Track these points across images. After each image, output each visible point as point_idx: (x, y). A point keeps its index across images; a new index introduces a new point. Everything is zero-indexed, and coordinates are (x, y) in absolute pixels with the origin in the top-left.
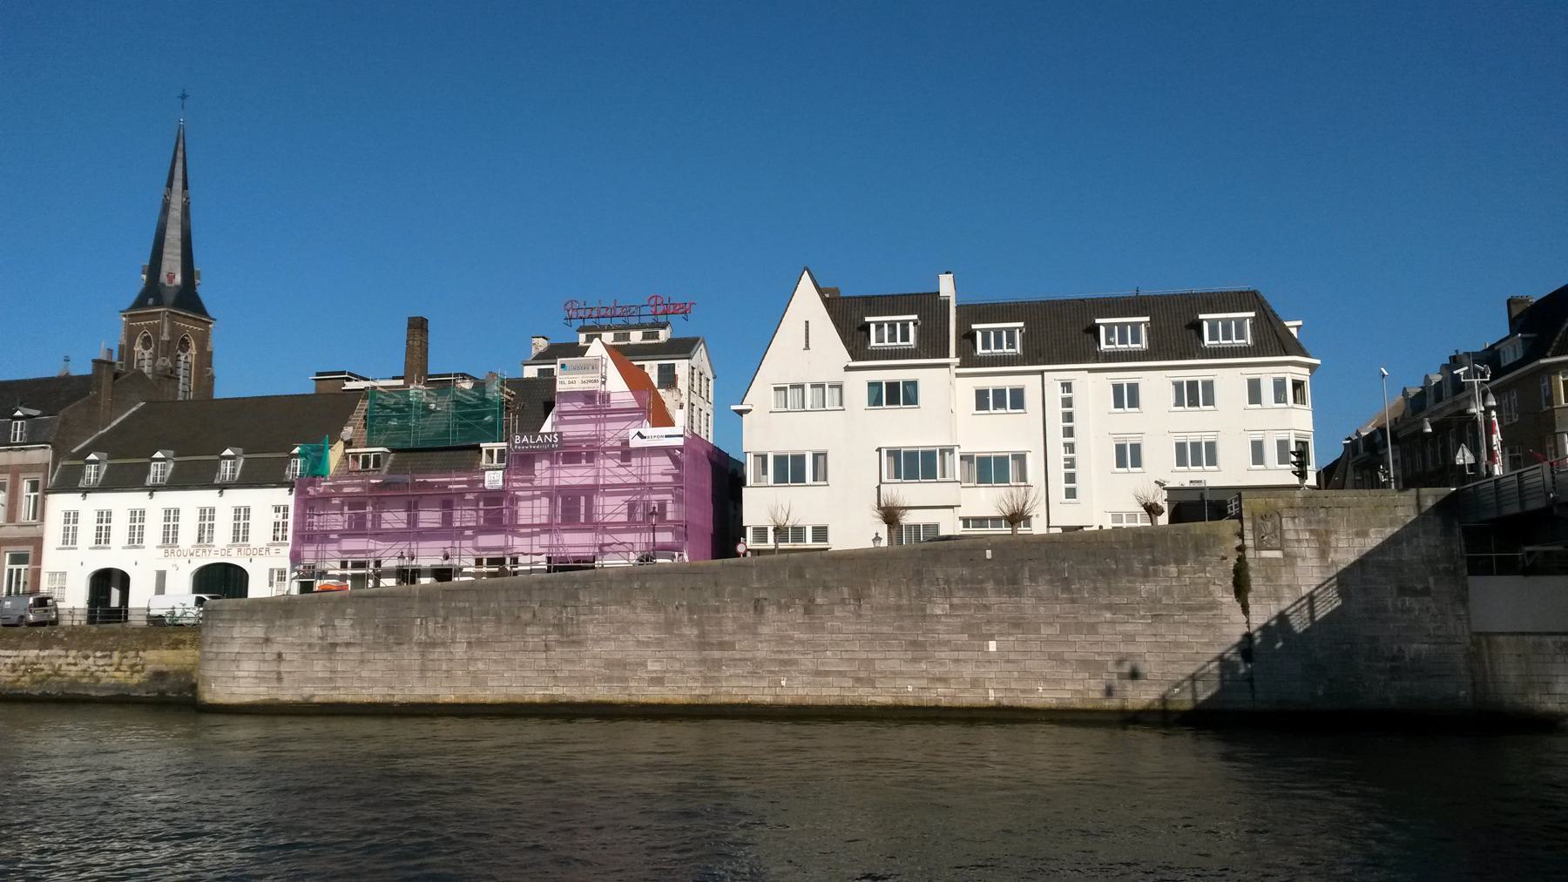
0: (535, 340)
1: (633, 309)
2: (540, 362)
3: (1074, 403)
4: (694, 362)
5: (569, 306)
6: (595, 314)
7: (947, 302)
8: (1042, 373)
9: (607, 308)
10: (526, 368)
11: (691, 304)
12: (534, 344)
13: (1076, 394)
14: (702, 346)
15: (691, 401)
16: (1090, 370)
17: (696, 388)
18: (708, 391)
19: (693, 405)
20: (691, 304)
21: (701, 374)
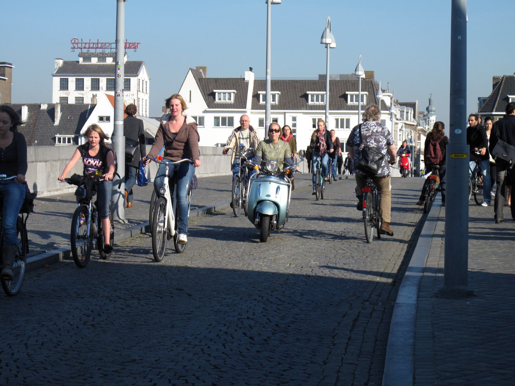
0: (57, 61)
1: (107, 45)
2: (61, 75)
3: (297, 125)
4: (139, 77)
5: (73, 42)
6: (87, 46)
7: (247, 84)
8: (285, 113)
9: (94, 44)
10: (54, 77)
11: (138, 44)
12: (56, 63)
13: (298, 122)
14: (144, 67)
15: (138, 97)
16: (304, 113)
17: (141, 89)
18: (146, 87)
19: (139, 98)
20: (138, 44)
21: (143, 81)
